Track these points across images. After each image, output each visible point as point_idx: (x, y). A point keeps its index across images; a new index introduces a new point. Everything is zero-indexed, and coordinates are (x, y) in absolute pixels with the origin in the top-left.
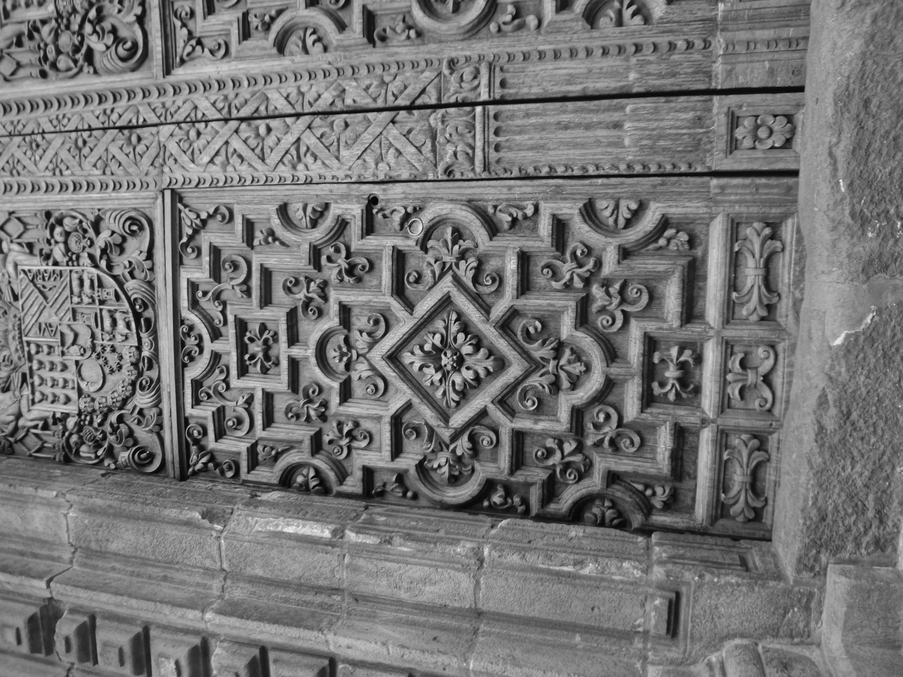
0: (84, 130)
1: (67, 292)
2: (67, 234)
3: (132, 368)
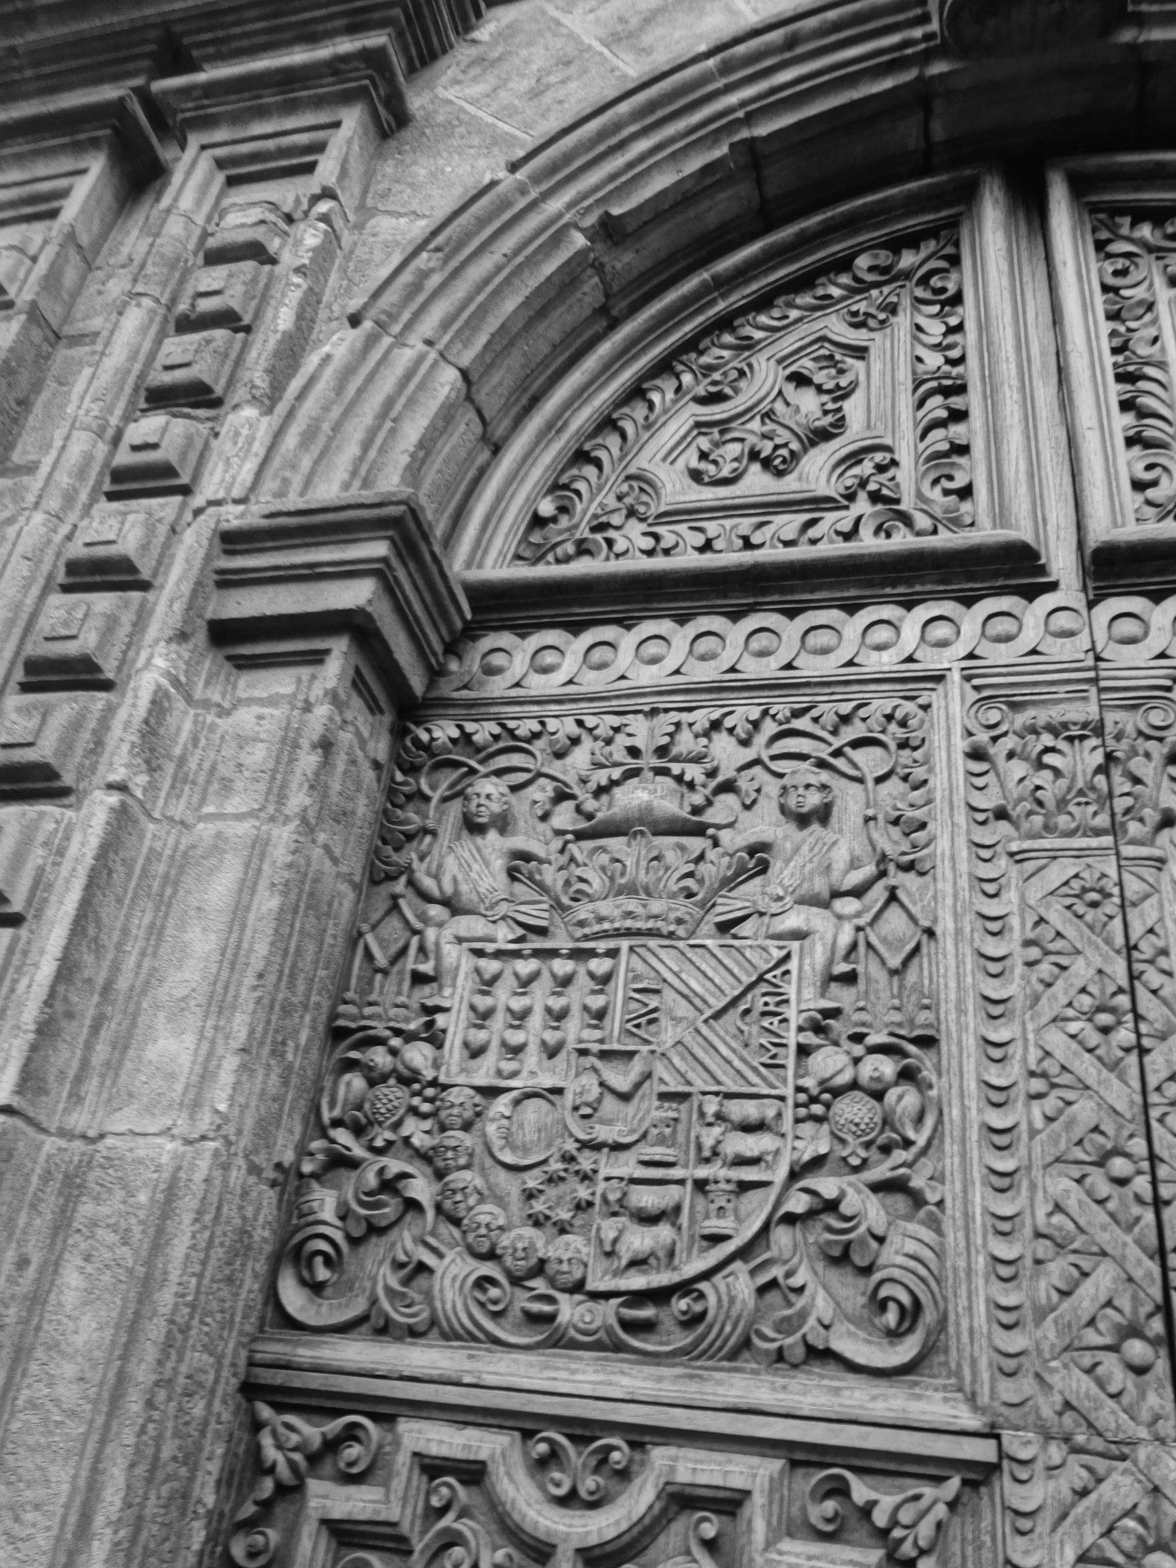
0: (1154, 1183)
1: (732, 1085)
2: (878, 1095)
3: (533, 1261)
